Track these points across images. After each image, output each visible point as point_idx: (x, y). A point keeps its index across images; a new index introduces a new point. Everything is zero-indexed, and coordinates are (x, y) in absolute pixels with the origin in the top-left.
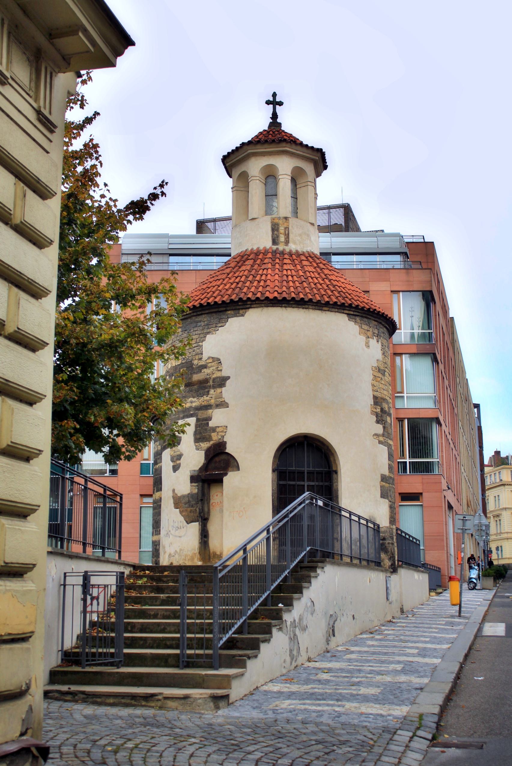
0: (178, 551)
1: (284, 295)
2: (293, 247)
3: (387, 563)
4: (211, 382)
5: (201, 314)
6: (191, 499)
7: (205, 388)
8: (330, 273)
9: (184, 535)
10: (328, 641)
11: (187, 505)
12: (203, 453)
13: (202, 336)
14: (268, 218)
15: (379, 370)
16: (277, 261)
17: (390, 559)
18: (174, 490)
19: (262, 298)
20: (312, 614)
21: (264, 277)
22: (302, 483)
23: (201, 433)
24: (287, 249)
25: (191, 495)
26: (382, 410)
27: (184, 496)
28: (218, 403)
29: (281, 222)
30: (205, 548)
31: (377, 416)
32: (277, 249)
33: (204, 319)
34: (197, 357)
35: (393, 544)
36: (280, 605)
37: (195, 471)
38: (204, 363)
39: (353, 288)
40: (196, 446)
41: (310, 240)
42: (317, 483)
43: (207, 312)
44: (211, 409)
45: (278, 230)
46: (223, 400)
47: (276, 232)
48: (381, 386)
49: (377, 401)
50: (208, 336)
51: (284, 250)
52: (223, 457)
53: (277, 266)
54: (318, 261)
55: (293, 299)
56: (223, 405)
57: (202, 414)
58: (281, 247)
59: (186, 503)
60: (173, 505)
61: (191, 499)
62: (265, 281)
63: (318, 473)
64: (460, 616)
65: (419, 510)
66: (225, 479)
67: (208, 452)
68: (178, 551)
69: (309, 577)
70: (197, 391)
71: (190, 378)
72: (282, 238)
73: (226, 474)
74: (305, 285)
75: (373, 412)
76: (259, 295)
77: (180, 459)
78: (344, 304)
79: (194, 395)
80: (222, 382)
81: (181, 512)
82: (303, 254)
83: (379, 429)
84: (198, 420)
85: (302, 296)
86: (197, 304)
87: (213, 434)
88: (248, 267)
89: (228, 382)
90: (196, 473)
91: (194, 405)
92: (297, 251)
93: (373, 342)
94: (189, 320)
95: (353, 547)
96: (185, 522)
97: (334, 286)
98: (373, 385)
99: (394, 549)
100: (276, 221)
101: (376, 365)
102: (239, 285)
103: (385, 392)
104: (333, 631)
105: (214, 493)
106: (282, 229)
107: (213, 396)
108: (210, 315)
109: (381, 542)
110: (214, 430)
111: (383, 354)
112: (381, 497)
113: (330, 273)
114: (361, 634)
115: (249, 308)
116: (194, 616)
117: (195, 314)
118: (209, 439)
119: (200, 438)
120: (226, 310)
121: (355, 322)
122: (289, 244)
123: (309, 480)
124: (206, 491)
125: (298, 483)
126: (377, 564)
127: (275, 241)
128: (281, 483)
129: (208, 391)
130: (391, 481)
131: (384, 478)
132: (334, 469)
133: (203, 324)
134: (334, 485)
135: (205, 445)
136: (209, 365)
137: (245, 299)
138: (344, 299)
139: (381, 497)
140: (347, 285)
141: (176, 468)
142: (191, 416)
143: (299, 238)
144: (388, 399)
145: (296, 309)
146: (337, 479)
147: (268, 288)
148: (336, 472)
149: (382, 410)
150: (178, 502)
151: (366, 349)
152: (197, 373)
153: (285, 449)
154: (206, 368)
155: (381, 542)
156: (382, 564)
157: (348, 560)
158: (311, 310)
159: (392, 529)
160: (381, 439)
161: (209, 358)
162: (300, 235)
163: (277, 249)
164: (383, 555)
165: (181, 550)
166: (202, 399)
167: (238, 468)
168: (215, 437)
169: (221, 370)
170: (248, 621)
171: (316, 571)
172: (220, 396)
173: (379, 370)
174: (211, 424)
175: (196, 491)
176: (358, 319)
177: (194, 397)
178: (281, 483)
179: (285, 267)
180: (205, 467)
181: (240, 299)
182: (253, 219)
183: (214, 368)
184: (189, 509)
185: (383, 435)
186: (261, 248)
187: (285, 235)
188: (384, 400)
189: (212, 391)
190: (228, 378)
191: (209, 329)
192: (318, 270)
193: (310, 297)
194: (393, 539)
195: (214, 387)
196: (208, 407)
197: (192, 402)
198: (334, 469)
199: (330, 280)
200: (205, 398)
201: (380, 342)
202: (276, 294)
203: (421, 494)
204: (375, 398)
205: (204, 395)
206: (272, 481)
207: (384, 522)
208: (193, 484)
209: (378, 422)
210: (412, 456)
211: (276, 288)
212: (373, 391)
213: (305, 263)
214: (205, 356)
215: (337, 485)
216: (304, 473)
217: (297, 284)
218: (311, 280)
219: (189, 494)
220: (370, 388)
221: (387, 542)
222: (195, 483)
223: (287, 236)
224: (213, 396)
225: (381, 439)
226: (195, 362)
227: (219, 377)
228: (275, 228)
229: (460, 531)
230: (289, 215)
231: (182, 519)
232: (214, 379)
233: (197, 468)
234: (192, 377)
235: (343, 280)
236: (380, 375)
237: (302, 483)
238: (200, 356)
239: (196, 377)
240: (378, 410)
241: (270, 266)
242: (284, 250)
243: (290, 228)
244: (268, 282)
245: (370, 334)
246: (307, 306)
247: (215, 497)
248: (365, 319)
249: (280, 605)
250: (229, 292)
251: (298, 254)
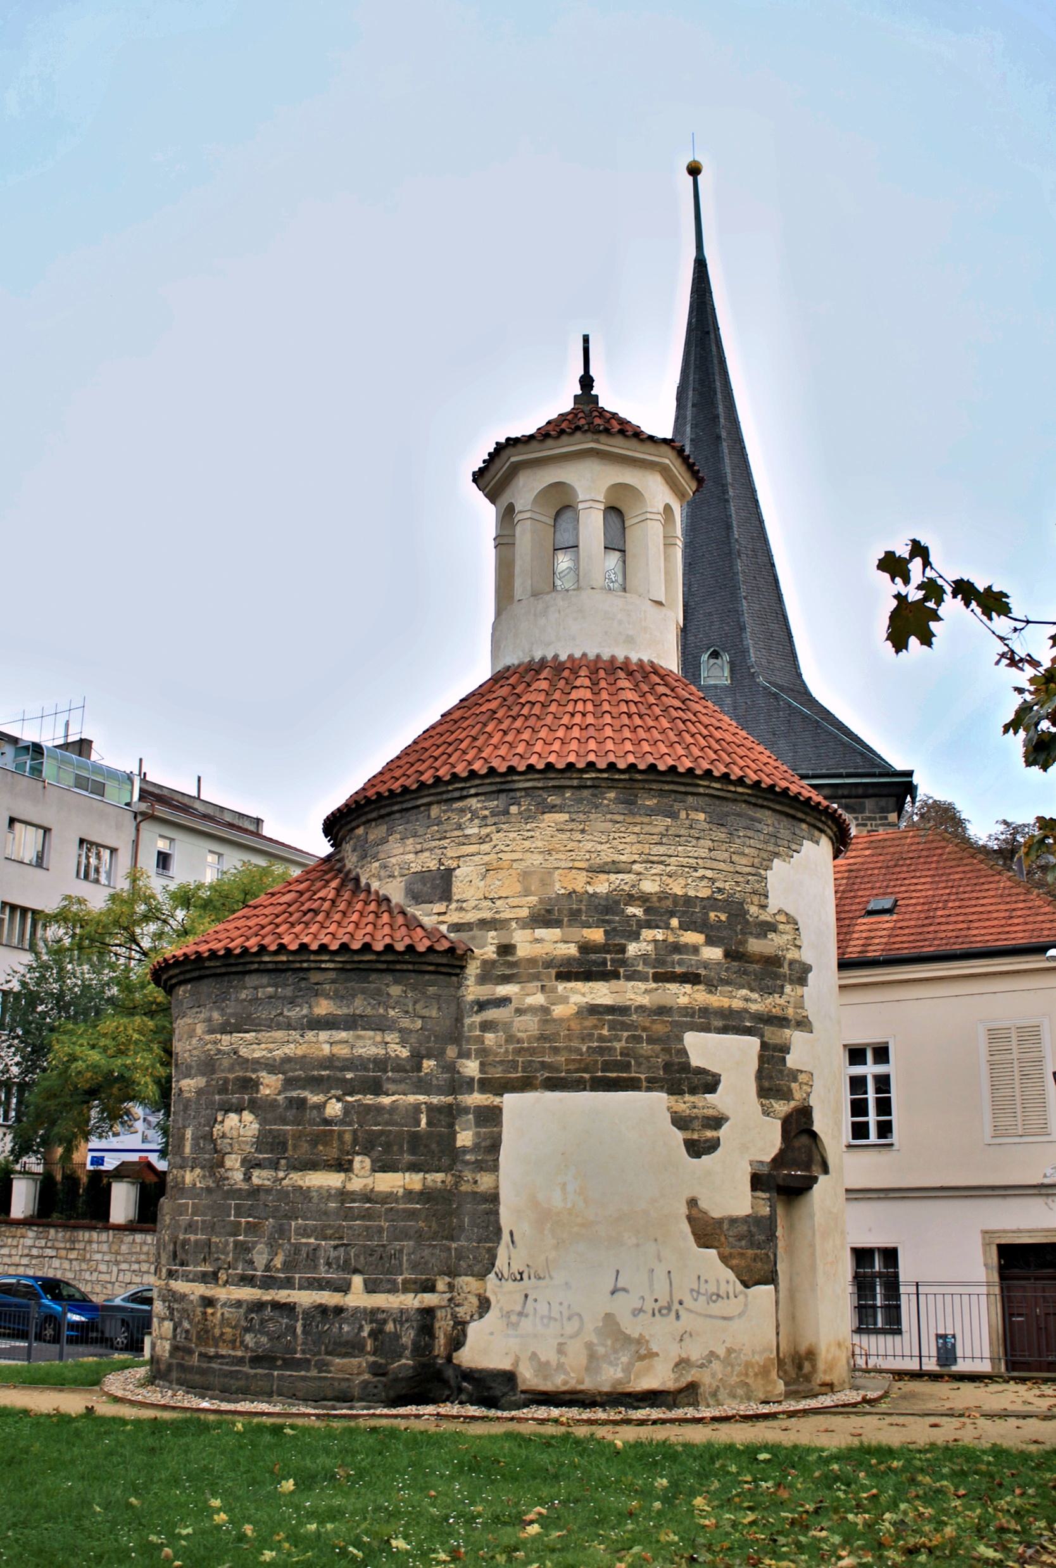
0: (722, 1352)
4: (786, 966)
5: (762, 806)
6: (753, 1229)
9: (740, 1315)
11: (743, 1243)
12: (779, 1123)
18: (692, 1203)
23: (771, 1077)
27: (733, 1221)
28: (799, 1018)
34: (756, 899)
37: (761, 1162)
38: (769, 919)
40: (762, 1105)
43: (778, 807)
44: (788, 1027)
57: (774, 1035)
59: (740, 1238)
61: (753, 1229)
67: (787, 1122)
68: (722, 1352)
70: (759, 978)
71: (743, 943)
79: (753, 984)
81: (724, 1259)
84: (764, 1046)
87: (793, 1085)
90: (765, 1170)
91: (754, 1007)
96: (738, 1282)
107: (792, 1000)
108: (778, 817)
110: (794, 1075)
117: (753, 800)
119: (770, 1089)
129: (782, 987)
135: (782, 1108)
142: (748, 1032)
152: (758, 936)
154: (775, 931)
165: (729, 1351)
169: (800, 947)
174: (792, 1061)
177: (752, 990)
183: (790, 937)
184: (750, 1252)
200: (776, 999)
205: (775, 992)
208: (759, 1194)
219: (748, 1216)
222: (763, 1191)
226: (753, 910)
231: (730, 1275)
232: (792, 963)
233: (768, 1158)
234: (746, 941)
239: (755, 945)
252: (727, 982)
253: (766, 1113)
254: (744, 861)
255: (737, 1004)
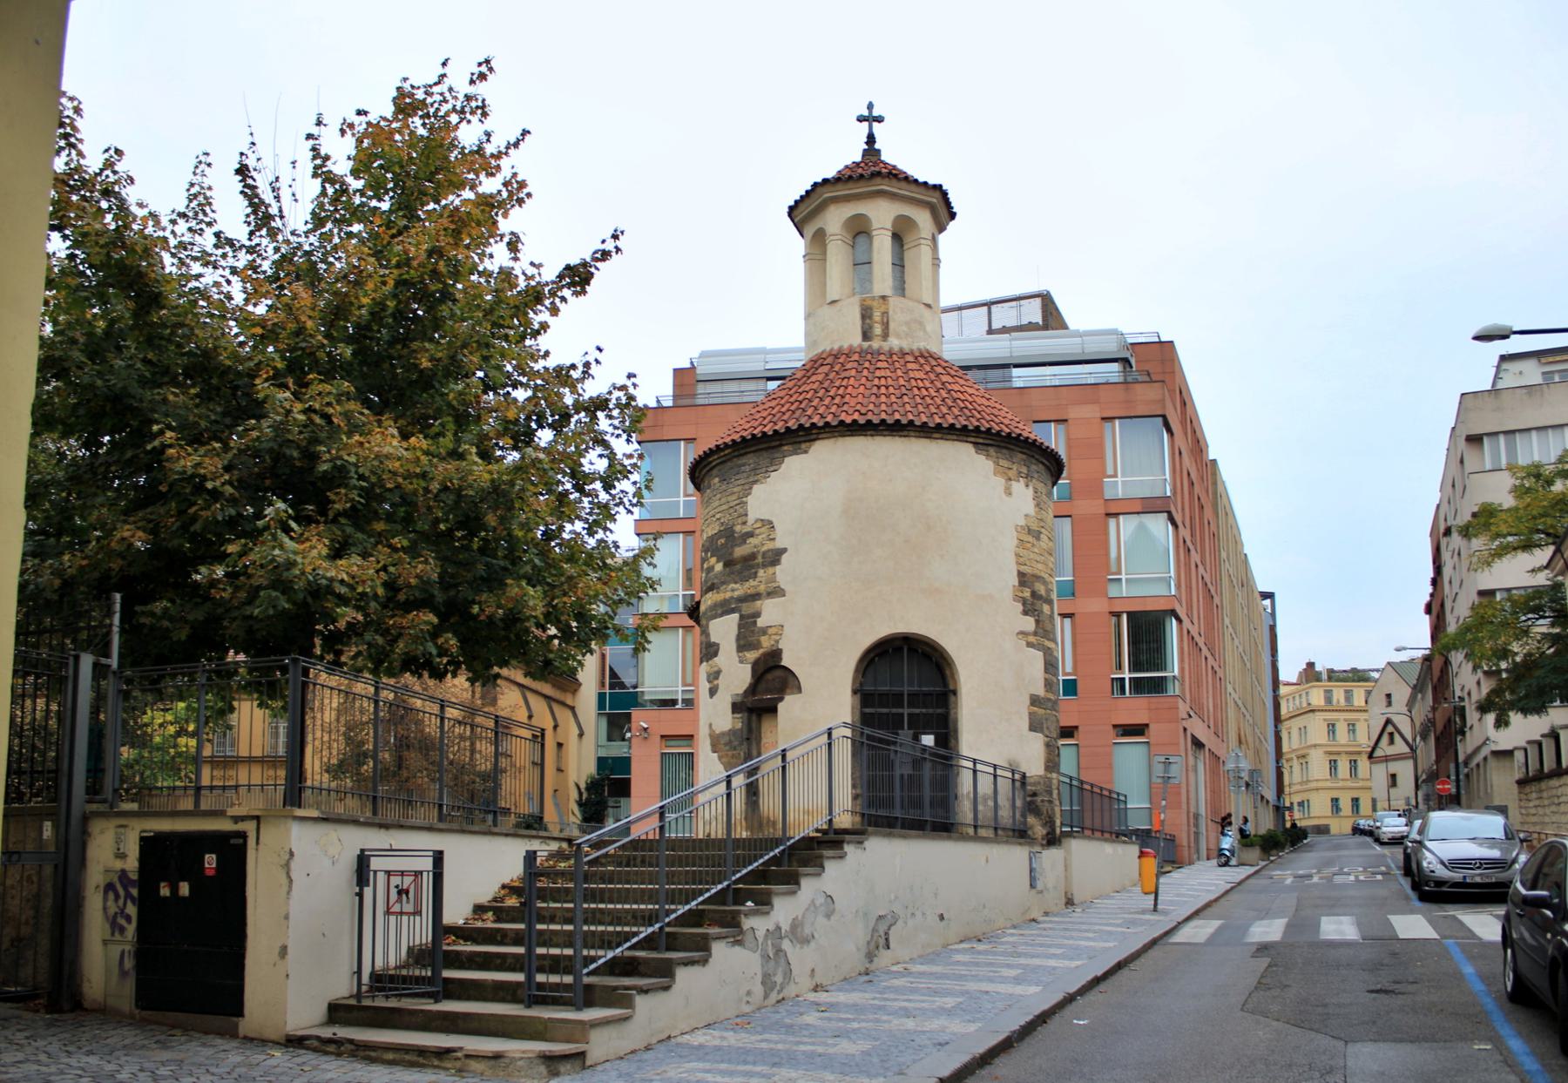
1: (870, 416)
2: (894, 343)
3: (1039, 831)
7: (753, 567)
8: (951, 380)
10: (870, 956)
12: (749, 667)
13: (747, 487)
14: (856, 301)
15: (1030, 531)
16: (867, 364)
17: (1044, 825)
19: (834, 423)
20: (828, 916)
21: (841, 391)
22: (900, 711)
24: (886, 346)
25: (732, 732)
26: (1034, 594)
27: (723, 734)
29: (875, 304)
30: (754, 810)
31: (1024, 604)
32: (870, 346)
33: (750, 460)
34: (740, 520)
35: (1050, 802)
36: (749, 903)
38: (749, 529)
39: (986, 403)
41: (925, 331)
42: (924, 711)
45: (870, 317)
46: (774, 585)
47: (868, 321)
48: (1032, 556)
49: (1023, 579)
50: (756, 488)
51: (881, 347)
52: (778, 673)
53: (865, 373)
54: (934, 363)
55: (883, 421)
56: (776, 592)
58: (876, 344)
59: (726, 744)
60: (709, 748)
62: (843, 397)
63: (926, 694)
64: (1155, 909)
65: (1142, 749)
66: (781, 706)
67: (755, 665)
69: (821, 857)
70: (740, 573)
71: (731, 554)
72: (878, 330)
73: (781, 699)
74: (906, 399)
75: (1016, 598)
76: (829, 418)
77: (717, 678)
78: (966, 426)
79: (737, 578)
80: (775, 557)
81: (720, 758)
82: (911, 353)
83: (1029, 623)
84: (742, 617)
85: (897, 416)
86: (736, 437)
88: (820, 377)
89: (784, 558)
90: (739, 699)
91: (736, 594)
92: (901, 350)
93: (1019, 487)
94: (729, 464)
95: (980, 808)
97: (955, 400)
98: (1018, 555)
99: (1053, 810)
100: (869, 303)
101: (1022, 522)
102: (802, 406)
103: (1040, 566)
104: (887, 940)
105: (766, 726)
106: (877, 316)
107: (763, 580)
109: (1028, 799)
110: (764, 631)
111: (1038, 505)
112: (1031, 730)
113: (951, 380)
114: (961, 941)
115: (815, 440)
116: (608, 919)
118: (756, 646)
120: (781, 445)
121: (988, 456)
122: (890, 339)
123: (911, 705)
124: (754, 725)
125: (894, 710)
126: (1020, 834)
127: (866, 336)
128: (867, 710)
130: (1050, 704)
131: (1035, 701)
132: (951, 687)
133: (747, 468)
134: (952, 712)
135: (752, 655)
136: (757, 531)
137: (807, 425)
138: (968, 418)
139: (1031, 730)
140: (978, 399)
141: (713, 692)
142: (733, 611)
143: (905, 328)
144: (1043, 575)
145: (888, 438)
146: (956, 703)
147: (845, 408)
148: (955, 693)
149: (1034, 594)
150: (718, 742)
151: (1004, 496)
152: (740, 545)
153: (872, 660)
155: (1028, 799)
156: (1030, 832)
157: (971, 831)
158: (913, 439)
159: (1050, 779)
160: (1032, 639)
161: (757, 521)
162: (907, 323)
163: (870, 346)
164: (1031, 820)
166: (747, 585)
167: (799, 690)
168: (766, 643)
170: (668, 929)
171: (842, 848)
172: (773, 579)
173: (1030, 531)
174: (761, 622)
175: (739, 725)
176: (992, 451)
178: (867, 710)
179: (878, 373)
180: (753, 689)
181: (801, 426)
182: (833, 302)
184: (730, 753)
185: (1035, 634)
186: (846, 345)
187: (883, 323)
188: (1038, 578)
189: (761, 572)
190: (784, 550)
191: (757, 475)
192: (932, 376)
193: (911, 417)
194: (1050, 793)
195: (764, 566)
196: (756, 596)
197: (733, 590)
198: (951, 687)
199: (949, 391)
200: (752, 583)
201: (1031, 488)
202: (856, 416)
203: (1147, 725)
204: (1021, 575)
206: (853, 708)
207: (1034, 766)
209: (1025, 613)
210: (1135, 666)
211: (859, 407)
212: (1018, 563)
213: (910, 366)
214: (751, 518)
215: (956, 713)
216: (902, 695)
217: (893, 398)
218: (916, 391)
220: (1013, 559)
221: (1039, 799)
223: (886, 326)
224: (763, 580)
225: (1032, 639)
226: (738, 528)
227: (772, 550)
228: (866, 314)
229: (1160, 780)
230: (888, 292)
232: (764, 553)
233: (741, 691)
235: (970, 391)
236: (1030, 539)
237: (900, 711)
238: (744, 518)
239: (739, 552)
240: (1027, 594)
241: (853, 373)
242: (881, 347)
243: (891, 313)
244: (847, 398)
245: (1011, 474)
246: (905, 433)
247: (769, 734)
248: (1004, 451)
249: (749, 903)
250: (785, 417)
251: (903, 354)
252: (723, 583)
253: (741, 662)
254: (735, 497)
255: (728, 595)
